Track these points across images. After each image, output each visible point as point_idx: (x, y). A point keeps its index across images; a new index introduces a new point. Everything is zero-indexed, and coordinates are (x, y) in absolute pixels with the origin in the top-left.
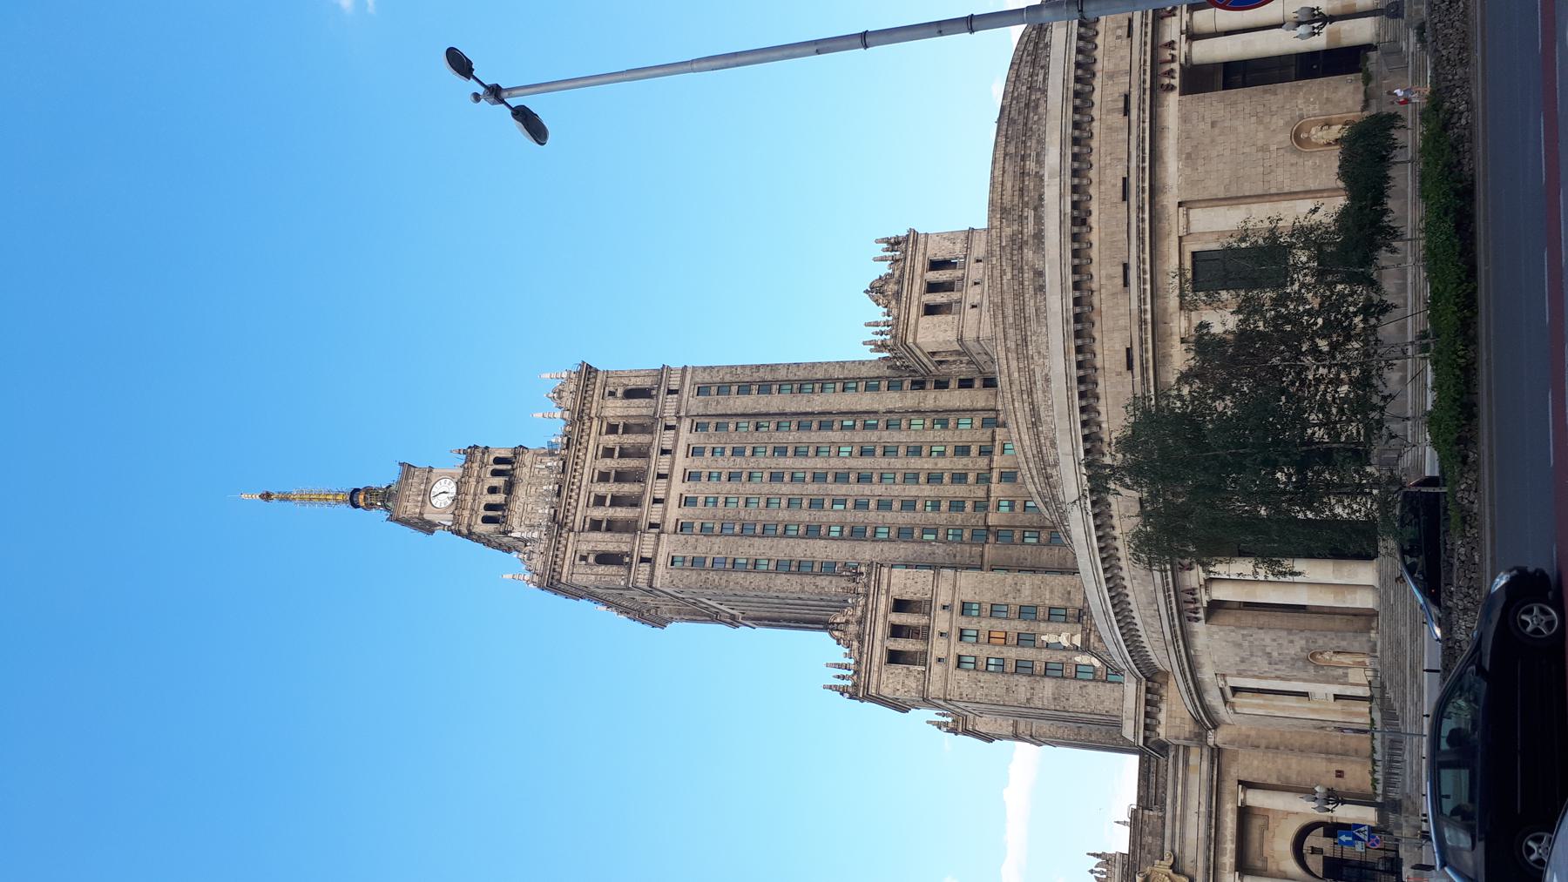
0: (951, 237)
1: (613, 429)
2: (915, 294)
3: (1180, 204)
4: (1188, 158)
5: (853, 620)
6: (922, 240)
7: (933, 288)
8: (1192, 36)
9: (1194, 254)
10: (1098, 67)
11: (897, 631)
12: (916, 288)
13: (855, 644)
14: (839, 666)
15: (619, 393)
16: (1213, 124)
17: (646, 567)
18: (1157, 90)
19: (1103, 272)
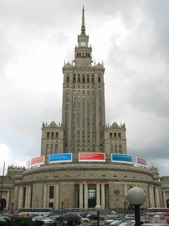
0: (125, 136)
1: (93, 76)
2: (114, 131)
3: (59, 184)
4: (65, 185)
5: (54, 126)
6: (124, 131)
7: (115, 134)
8: (84, 186)
10: (86, 171)
11: (53, 133)
12: (115, 131)
13: (50, 127)
14: (47, 124)
15: (99, 76)
16: (70, 189)
17: (67, 86)
18: (75, 180)
19: (56, 173)
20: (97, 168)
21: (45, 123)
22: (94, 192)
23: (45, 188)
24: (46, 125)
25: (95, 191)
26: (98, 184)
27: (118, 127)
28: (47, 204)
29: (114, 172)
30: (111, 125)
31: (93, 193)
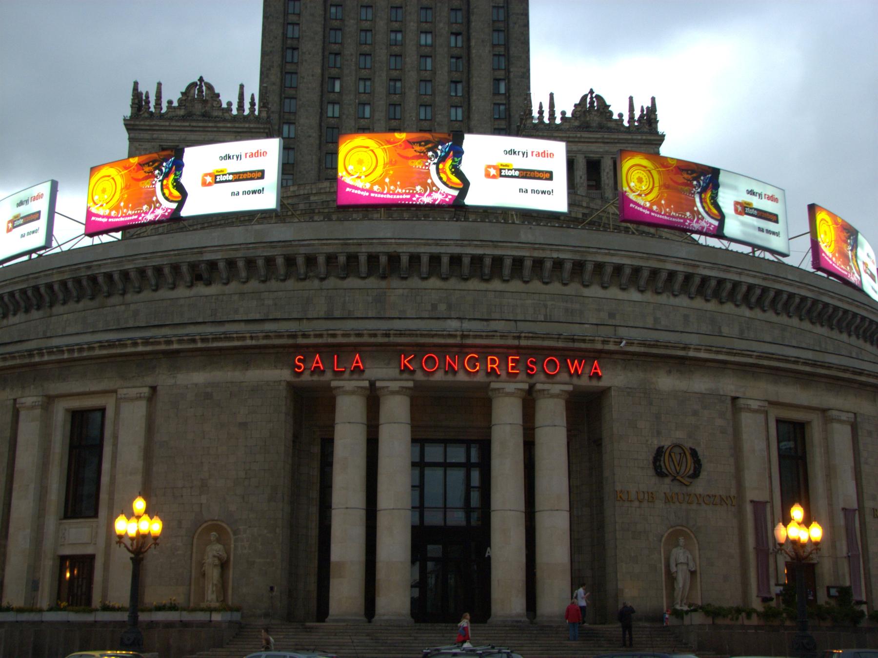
3: (154, 389)
9: (103, 410)
10: (395, 282)
12: (593, 147)
13: (182, 112)
16: (243, 425)
20: (498, 261)
21: (148, 88)
22: (468, 466)
23: (29, 430)
24: (152, 104)
25: (474, 458)
26: (511, 387)
27: (612, 125)
28: (34, 568)
29: (649, 296)
30: (566, 105)
31: (457, 476)
